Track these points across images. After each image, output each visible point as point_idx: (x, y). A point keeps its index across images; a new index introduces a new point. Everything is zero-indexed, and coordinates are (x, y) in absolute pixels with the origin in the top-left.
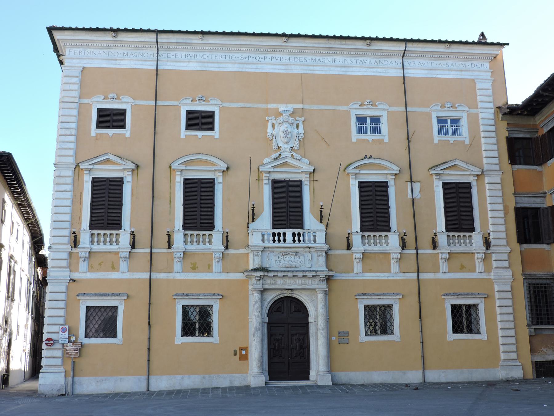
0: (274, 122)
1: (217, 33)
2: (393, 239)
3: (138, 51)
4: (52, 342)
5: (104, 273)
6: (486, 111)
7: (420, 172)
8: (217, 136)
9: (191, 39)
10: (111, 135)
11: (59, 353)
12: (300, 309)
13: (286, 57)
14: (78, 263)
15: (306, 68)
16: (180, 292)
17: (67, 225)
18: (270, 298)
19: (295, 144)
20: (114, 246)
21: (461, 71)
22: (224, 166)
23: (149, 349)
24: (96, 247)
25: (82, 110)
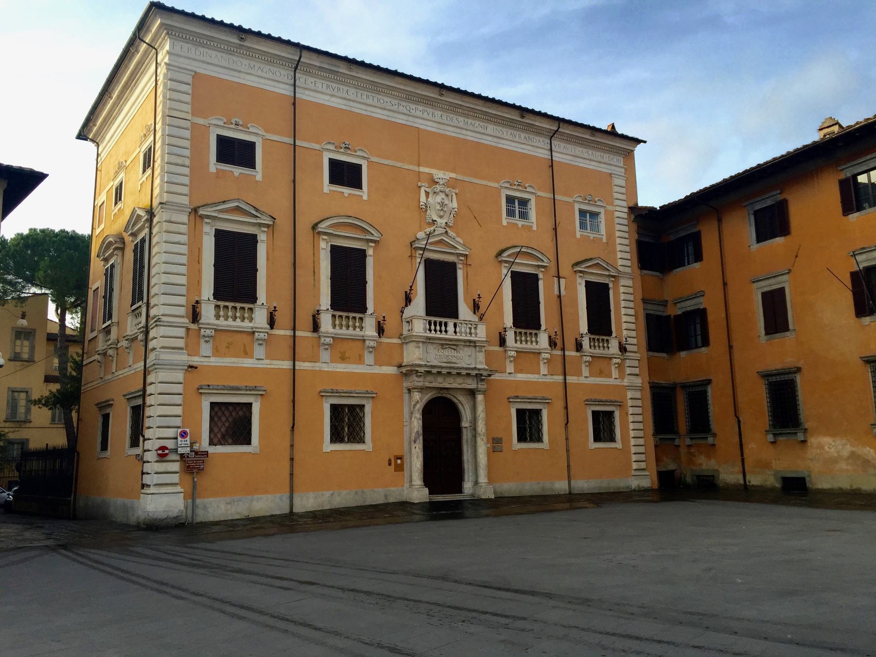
0: (427, 190)
1: (370, 67)
3: (268, 67)
4: (167, 452)
5: (233, 360)
9: (339, 67)
10: (236, 174)
11: (176, 467)
14: (198, 344)
15: (458, 130)
16: (328, 388)
17: (183, 290)
20: (247, 324)
21: (600, 162)
23: (292, 459)
24: (222, 322)
25: (198, 133)
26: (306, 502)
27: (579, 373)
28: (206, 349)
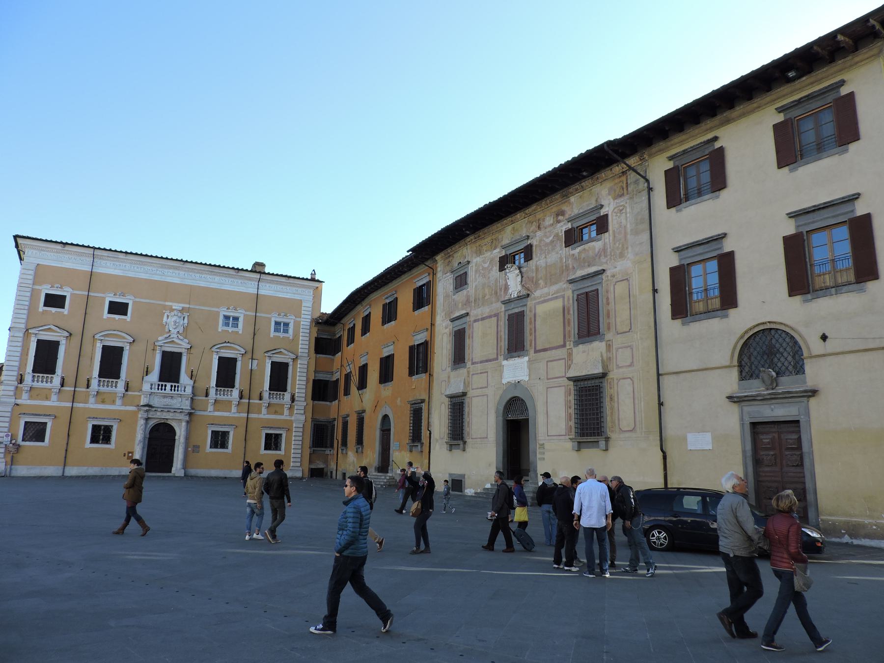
2: (235, 393)
6: (306, 320)
7: (258, 354)
8: (128, 320)
12: (171, 431)
13: (182, 273)
17: (16, 369)
18: (152, 423)
19: (181, 330)
22: (131, 340)
24: (35, 384)
25: (34, 294)
26: (72, 471)
27: (260, 412)
28: (25, 396)
